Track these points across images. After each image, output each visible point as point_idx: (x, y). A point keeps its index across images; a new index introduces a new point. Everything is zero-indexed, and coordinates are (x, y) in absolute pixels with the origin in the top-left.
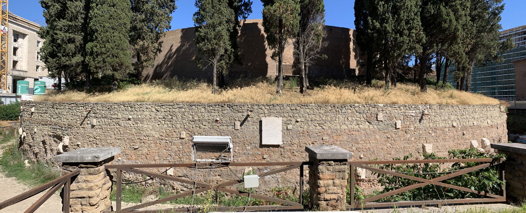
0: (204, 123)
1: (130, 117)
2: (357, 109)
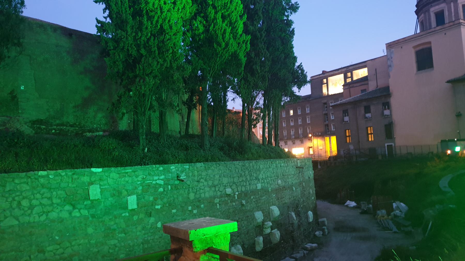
2: (42, 180)
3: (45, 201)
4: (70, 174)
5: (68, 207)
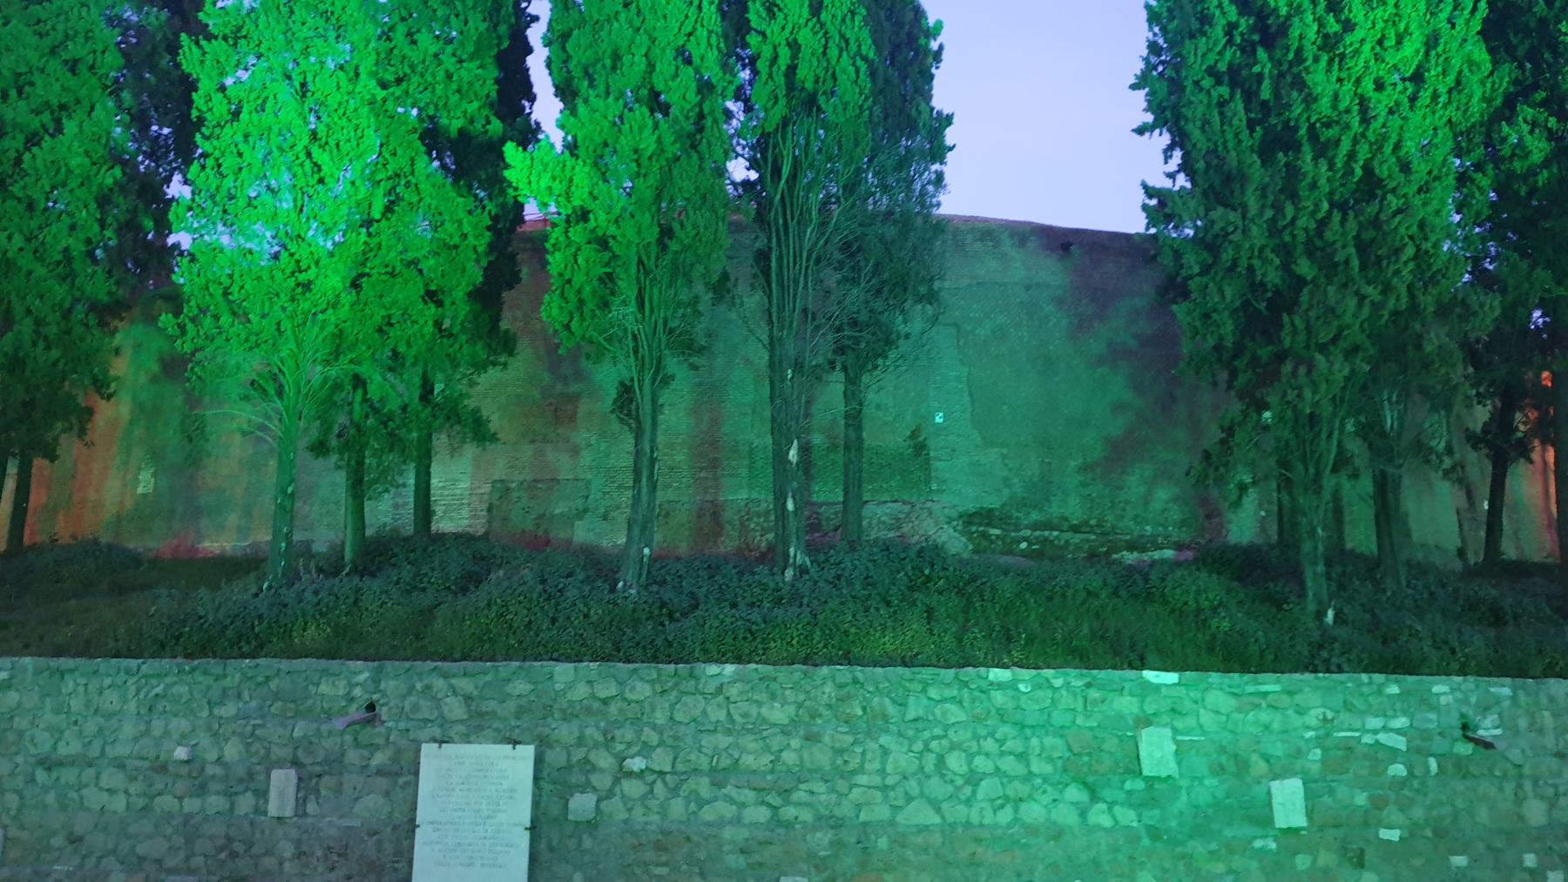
0: (112, 778)
2: (999, 697)
3: (1009, 764)
4: (1078, 683)
5: (1074, 793)
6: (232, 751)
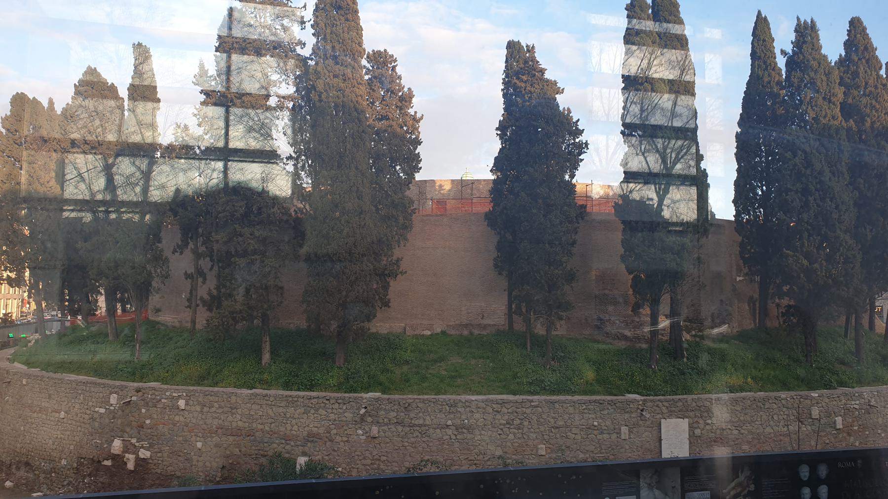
0: (574, 430)
1: (449, 423)
6: (608, 423)
